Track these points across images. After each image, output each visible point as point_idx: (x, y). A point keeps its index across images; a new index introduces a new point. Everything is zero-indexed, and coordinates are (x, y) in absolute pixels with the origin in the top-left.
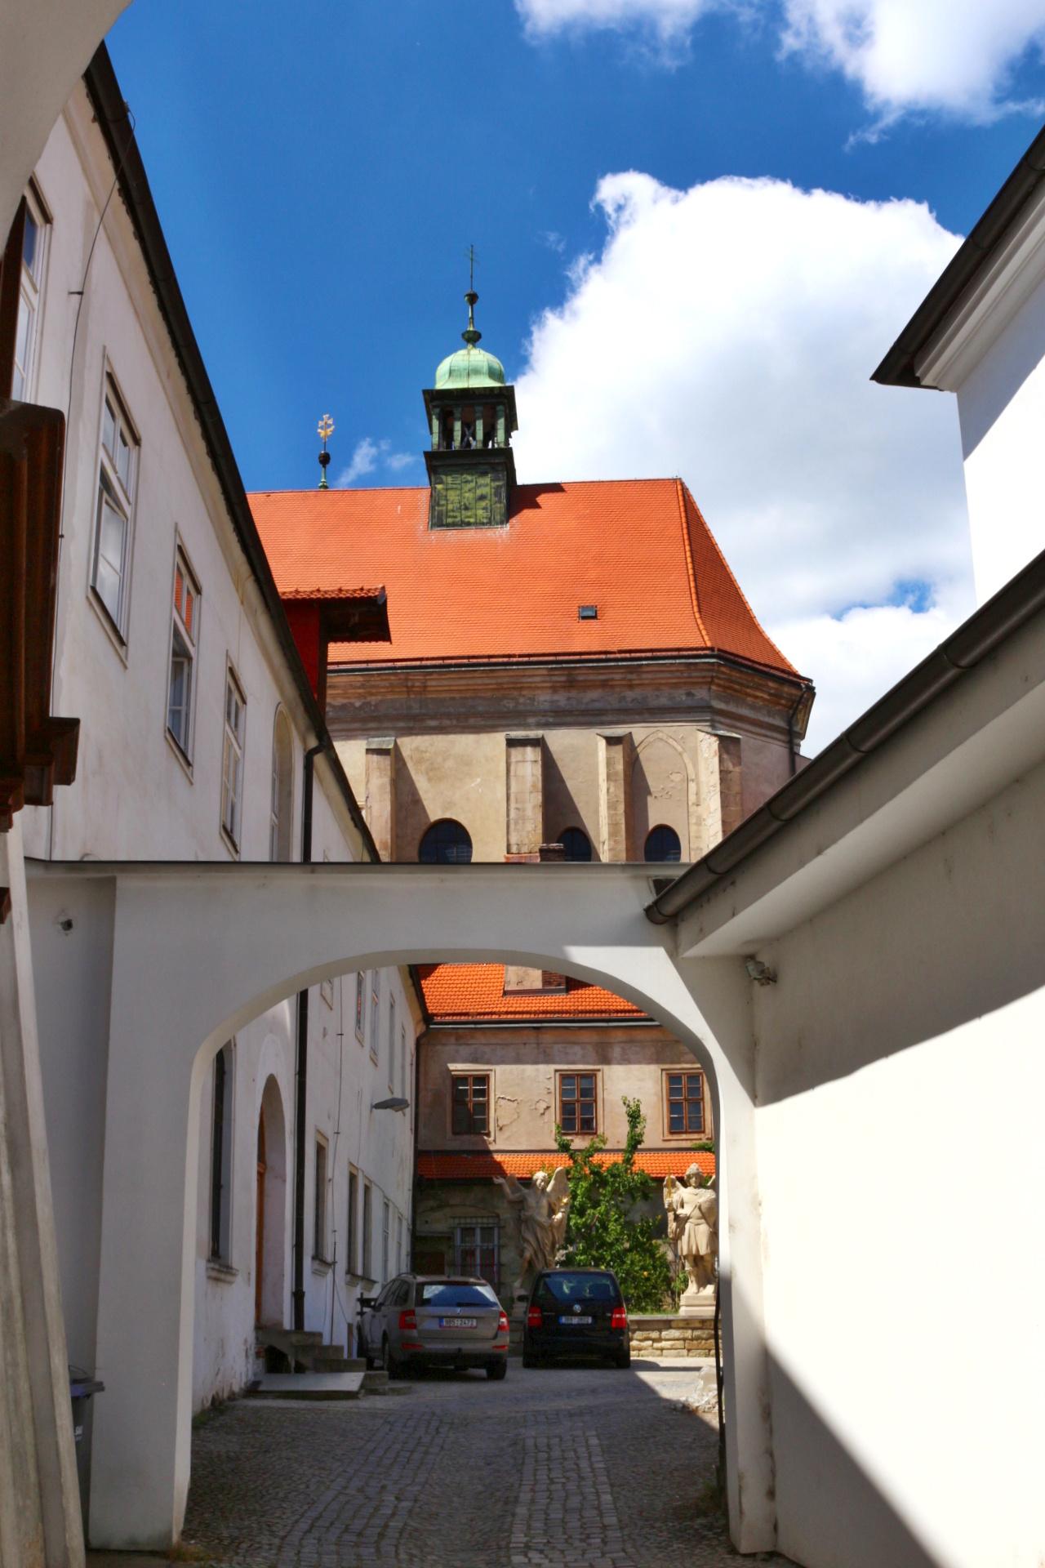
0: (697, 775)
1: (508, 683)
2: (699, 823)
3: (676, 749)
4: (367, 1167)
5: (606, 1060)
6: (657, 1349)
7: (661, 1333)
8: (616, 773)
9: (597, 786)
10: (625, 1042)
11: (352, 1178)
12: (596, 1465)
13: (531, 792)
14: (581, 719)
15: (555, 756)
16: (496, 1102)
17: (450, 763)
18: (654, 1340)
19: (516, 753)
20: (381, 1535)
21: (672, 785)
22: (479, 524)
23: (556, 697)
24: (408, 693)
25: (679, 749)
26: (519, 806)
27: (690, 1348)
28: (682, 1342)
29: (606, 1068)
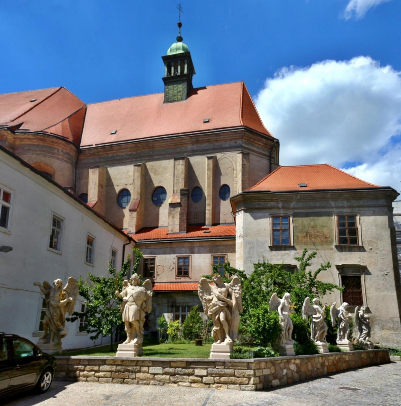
0: (236, 168)
1: (179, 143)
2: (236, 183)
3: (230, 160)
5: (193, 253)
6: (97, 377)
7: (99, 368)
8: (210, 168)
9: (205, 173)
10: (200, 246)
13: (181, 174)
14: (201, 153)
15: (192, 165)
16: (157, 267)
17: (161, 169)
18: (96, 371)
19: (177, 162)
21: (229, 171)
23: (193, 147)
24: (149, 148)
25: (231, 160)
26: (177, 178)
27: (114, 377)
28: (109, 373)
29: (193, 255)
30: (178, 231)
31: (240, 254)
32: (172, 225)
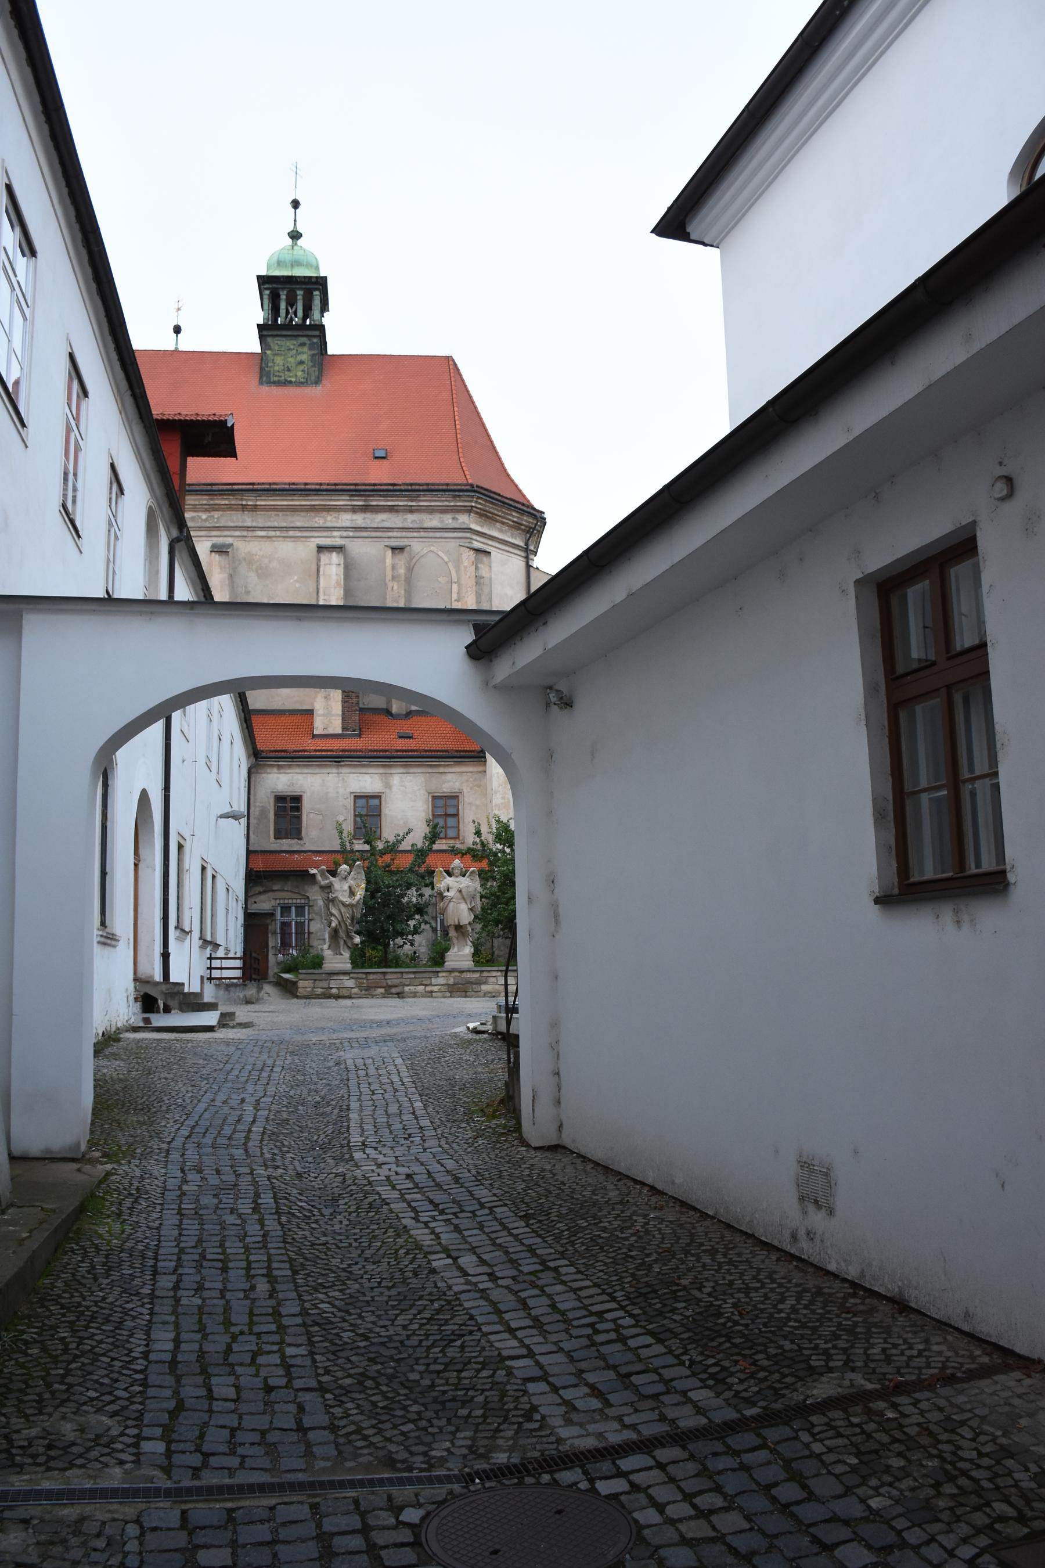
4: (213, 863)
8: (399, 576)
11: (203, 869)
12: (405, 1080)
19: (324, 558)
20: (247, 1138)
22: (299, 384)
25: (446, 559)
30: (339, 731)
31: (503, 798)
32: (323, 715)
